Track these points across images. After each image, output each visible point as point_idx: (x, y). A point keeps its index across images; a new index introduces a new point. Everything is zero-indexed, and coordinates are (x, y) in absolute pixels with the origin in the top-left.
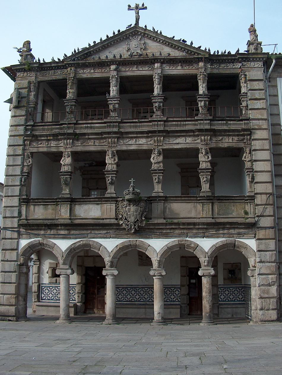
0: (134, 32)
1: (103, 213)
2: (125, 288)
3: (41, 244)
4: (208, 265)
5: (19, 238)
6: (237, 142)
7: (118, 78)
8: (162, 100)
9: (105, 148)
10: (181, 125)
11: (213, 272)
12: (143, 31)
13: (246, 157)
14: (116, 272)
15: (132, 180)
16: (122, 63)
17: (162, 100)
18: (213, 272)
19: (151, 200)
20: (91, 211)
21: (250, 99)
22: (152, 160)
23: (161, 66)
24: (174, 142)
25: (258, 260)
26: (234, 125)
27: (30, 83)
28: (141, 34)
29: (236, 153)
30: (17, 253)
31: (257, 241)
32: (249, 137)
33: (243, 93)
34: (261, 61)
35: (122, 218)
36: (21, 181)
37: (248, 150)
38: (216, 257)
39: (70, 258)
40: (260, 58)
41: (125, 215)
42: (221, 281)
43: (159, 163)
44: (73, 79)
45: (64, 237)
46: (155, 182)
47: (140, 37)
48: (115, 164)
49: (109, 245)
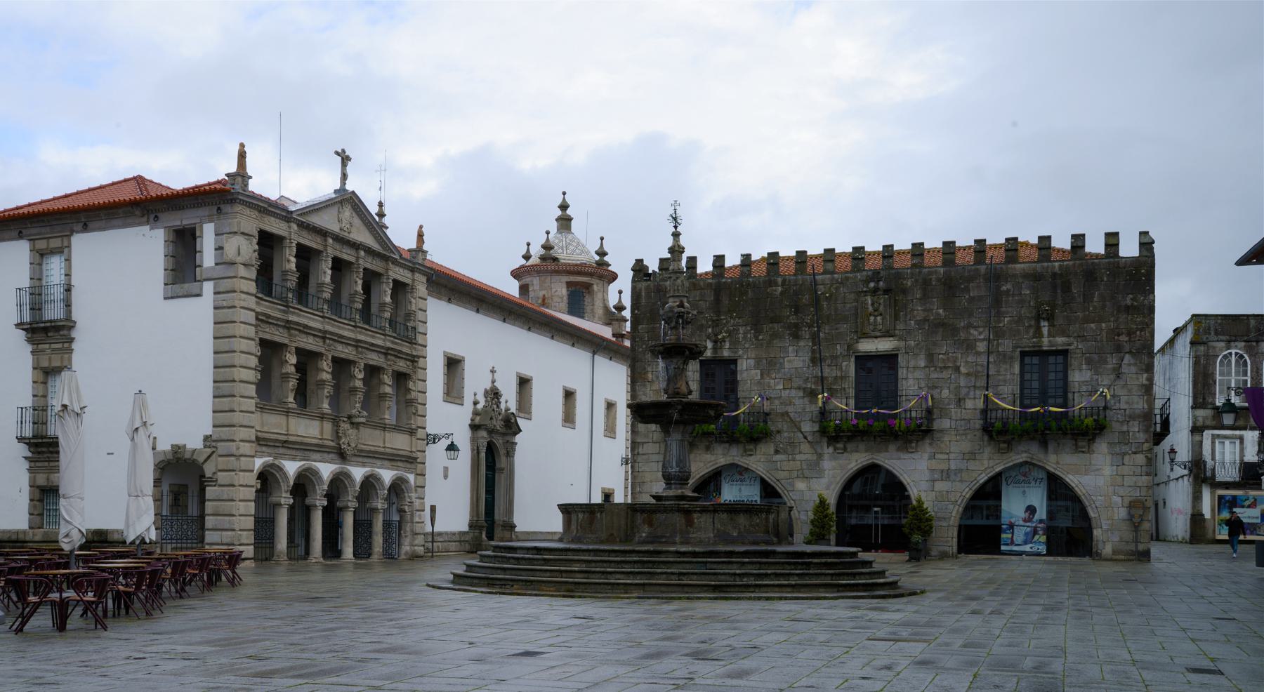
1: (322, 433)
9: (323, 350)
16: (338, 239)
45: (293, 458)
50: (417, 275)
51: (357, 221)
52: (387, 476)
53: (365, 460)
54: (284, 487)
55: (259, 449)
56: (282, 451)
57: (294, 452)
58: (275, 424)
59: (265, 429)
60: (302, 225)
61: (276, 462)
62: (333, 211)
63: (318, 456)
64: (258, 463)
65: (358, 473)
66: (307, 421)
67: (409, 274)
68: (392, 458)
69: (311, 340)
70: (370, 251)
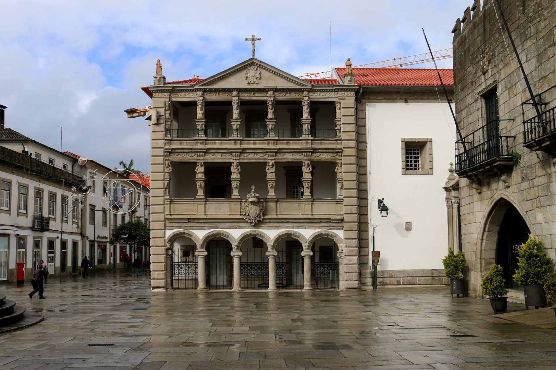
1: (230, 210)
2: (248, 264)
3: (184, 233)
4: (308, 249)
5: (165, 229)
8: (274, 123)
9: (231, 160)
10: (289, 143)
11: (311, 254)
13: (338, 169)
14: (241, 254)
15: (253, 187)
16: (240, 90)
17: (274, 123)
18: (311, 254)
21: (343, 124)
22: (267, 170)
23: (273, 94)
25: (345, 245)
27: (165, 103)
29: (331, 166)
30: (165, 240)
36: (164, 184)
37: (340, 164)
38: (314, 243)
40: (352, 89)
41: (248, 212)
42: (317, 260)
43: (272, 173)
45: (202, 228)
46: (269, 187)
47: (256, 67)
48: (239, 173)
49: (235, 234)
50: (340, 94)
52: (307, 234)
53: (281, 224)
54: (199, 246)
55: (168, 224)
56: (189, 224)
57: (203, 225)
58: (184, 209)
61: (186, 231)
62: (242, 74)
63: (223, 225)
64: (169, 233)
65: (271, 234)
66: (217, 205)
67: (334, 94)
68: (312, 222)
69: (219, 155)
70: (276, 90)
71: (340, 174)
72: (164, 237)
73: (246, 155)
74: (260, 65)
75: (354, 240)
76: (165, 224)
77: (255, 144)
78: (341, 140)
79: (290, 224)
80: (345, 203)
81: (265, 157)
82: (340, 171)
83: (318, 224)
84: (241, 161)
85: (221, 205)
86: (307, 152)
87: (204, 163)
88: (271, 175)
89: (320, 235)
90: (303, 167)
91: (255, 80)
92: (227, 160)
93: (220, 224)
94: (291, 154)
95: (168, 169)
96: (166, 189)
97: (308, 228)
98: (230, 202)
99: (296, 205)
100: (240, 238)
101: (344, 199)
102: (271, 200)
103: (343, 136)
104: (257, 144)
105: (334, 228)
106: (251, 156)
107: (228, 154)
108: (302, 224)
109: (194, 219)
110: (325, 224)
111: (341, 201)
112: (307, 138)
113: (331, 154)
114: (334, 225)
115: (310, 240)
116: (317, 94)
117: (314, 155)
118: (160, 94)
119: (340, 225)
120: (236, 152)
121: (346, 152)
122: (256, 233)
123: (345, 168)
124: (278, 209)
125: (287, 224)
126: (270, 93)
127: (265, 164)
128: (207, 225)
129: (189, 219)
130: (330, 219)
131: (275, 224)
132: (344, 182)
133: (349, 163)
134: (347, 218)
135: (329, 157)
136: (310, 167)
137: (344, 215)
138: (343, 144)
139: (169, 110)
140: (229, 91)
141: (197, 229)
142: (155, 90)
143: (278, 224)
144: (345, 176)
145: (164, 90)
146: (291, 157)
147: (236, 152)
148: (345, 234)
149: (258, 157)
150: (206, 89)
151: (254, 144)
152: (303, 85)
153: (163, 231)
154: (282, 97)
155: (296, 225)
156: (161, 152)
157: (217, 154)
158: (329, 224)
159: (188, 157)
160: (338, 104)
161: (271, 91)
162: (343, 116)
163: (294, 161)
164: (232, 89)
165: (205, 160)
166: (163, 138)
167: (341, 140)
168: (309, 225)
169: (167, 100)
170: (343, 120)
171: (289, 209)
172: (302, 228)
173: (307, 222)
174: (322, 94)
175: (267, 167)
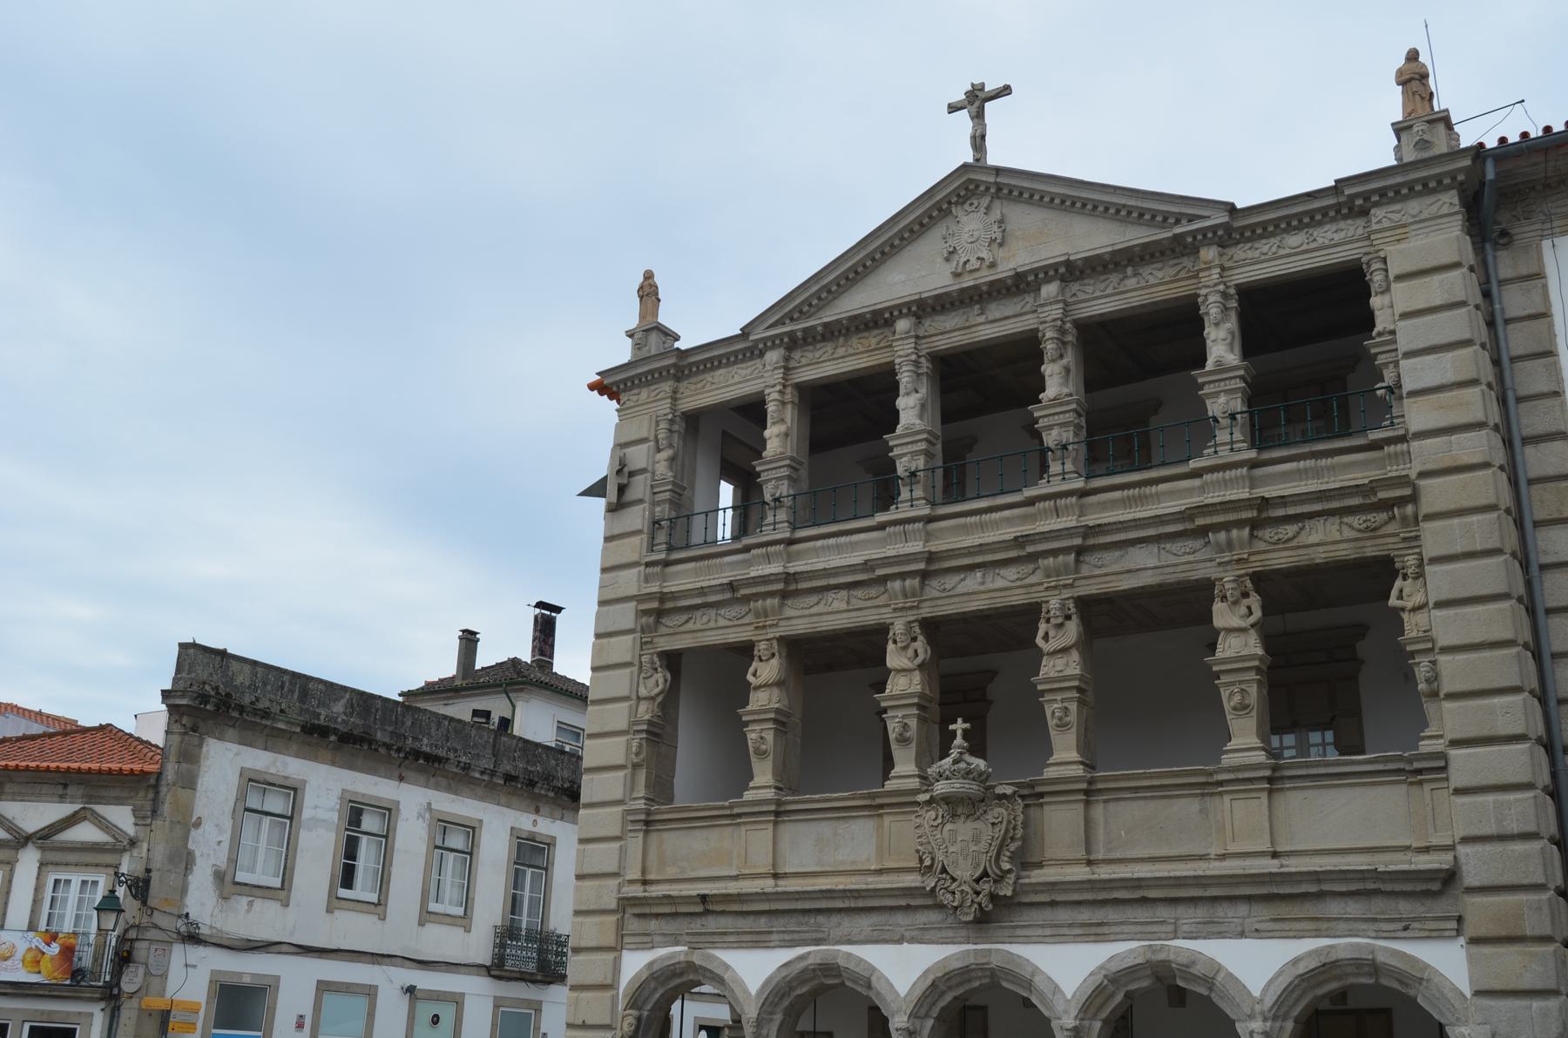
0: (976, 186)
5: (616, 949)
6: (1360, 535)
7: (922, 360)
12: (991, 179)
13: (1404, 594)
19: (1042, 795)
20: (840, 847)
22: (1039, 641)
23: (1062, 290)
24: (1117, 568)
26: (1349, 471)
28: (988, 189)
30: (614, 999)
31: (1475, 949)
32: (1410, 509)
33: (1380, 334)
34: (1449, 188)
35: (932, 866)
37: (1411, 560)
39: (778, 1017)
40: (1439, 179)
41: (940, 856)
43: (1064, 650)
44: (778, 388)
45: (758, 941)
47: (985, 201)
48: (921, 667)
51: (1023, 218)
53: (1111, 914)
55: (633, 925)
56: (712, 924)
57: (762, 923)
59: (671, 872)
60: (793, 343)
61: (697, 958)
62: (931, 246)
63: (847, 924)
66: (825, 829)
67: (1354, 228)
68: (1277, 896)
69: (838, 601)
70: (1072, 271)
71: (1421, 618)
72: (610, 986)
73: (950, 581)
74: (999, 188)
75: (1536, 1004)
76: (620, 925)
77: (987, 524)
78: (1402, 439)
79: (1163, 912)
80: (1458, 778)
81: (1033, 579)
82: (1419, 599)
83: (1311, 909)
84: (926, 611)
85: (842, 827)
86: (1226, 526)
87: (781, 640)
88: (1059, 662)
89: (1328, 968)
90: (1218, 607)
91: (983, 255)
92: (870, 618)
93: (835, 919)
94: (1154, 548)
95: (652, 681)
96: (636, 766)
97: (1258, 934)
98: (876, 809)
99: (1187, 808)
100: (918, 992)
101: (1454, 753)
102: (1062, 790)
103: (1417, 416)
104: (996, 524)
105: (1406, 929)
106: (972, 582)
107: (873, 592)
108: (1223, 911)
109: (727, 898)
110: (1354, 908)
111: (1438, 767)
112: (1225, 456)
113: (1356, 521)
114: (1405, 908)
115: (1269, 1001)
116: (1266, 247)
117: (1268, 533)
118: (644, 394)
119: (1442, 907)
120: (903, 576)
121: (1435, 494)
122: (995, 962)
123: (1441, 582)
124: (1100, 835)
125: (1142, 914)
126: (1050, 290)
127: (1030, 614)
128: (779, 924)
129: (704, 898)
130: (1375, 874)
131: (1085, 915)
132: (1443, 659)
133: (1459, 549)
134: (1476, 865)
135: (1348, 533)
136: (1255, 601)
137: (1463, 850)
138: (1425, 453)
139: (670, 446)
140: (879, 320)
141: (740, 945)
142: (624, 381)
143: (1099, 915)
144: (1448, 627)
145: (651, 372)
146: (1152, 562)
147: (903, 576)
148: (1471, 960)
149: (1000, 583)
150: (791, 334)
151: (982, 526)
152: (1192, 218)
153: (610, 956)
154: (1104, 300)
155: (1189, 916)
156: (626, 616)
157: (831, 595)
158: (1377, 906)
159: (722, 622)
160: (1379, 265)
161: (1049, 280)
162: (1405, 316)
163: (1171, 578)
164: (890, 309)
165: (785, 629)
166: (635, 557)
167: (1402, 439)
168: (1263, 912)
169: (664, 407)
170: (1409, 335)
171: (1152, 832)
172: (1221, 935)
173: (1249, 899)
174: (1294, 240)
175: (1043, 627)
